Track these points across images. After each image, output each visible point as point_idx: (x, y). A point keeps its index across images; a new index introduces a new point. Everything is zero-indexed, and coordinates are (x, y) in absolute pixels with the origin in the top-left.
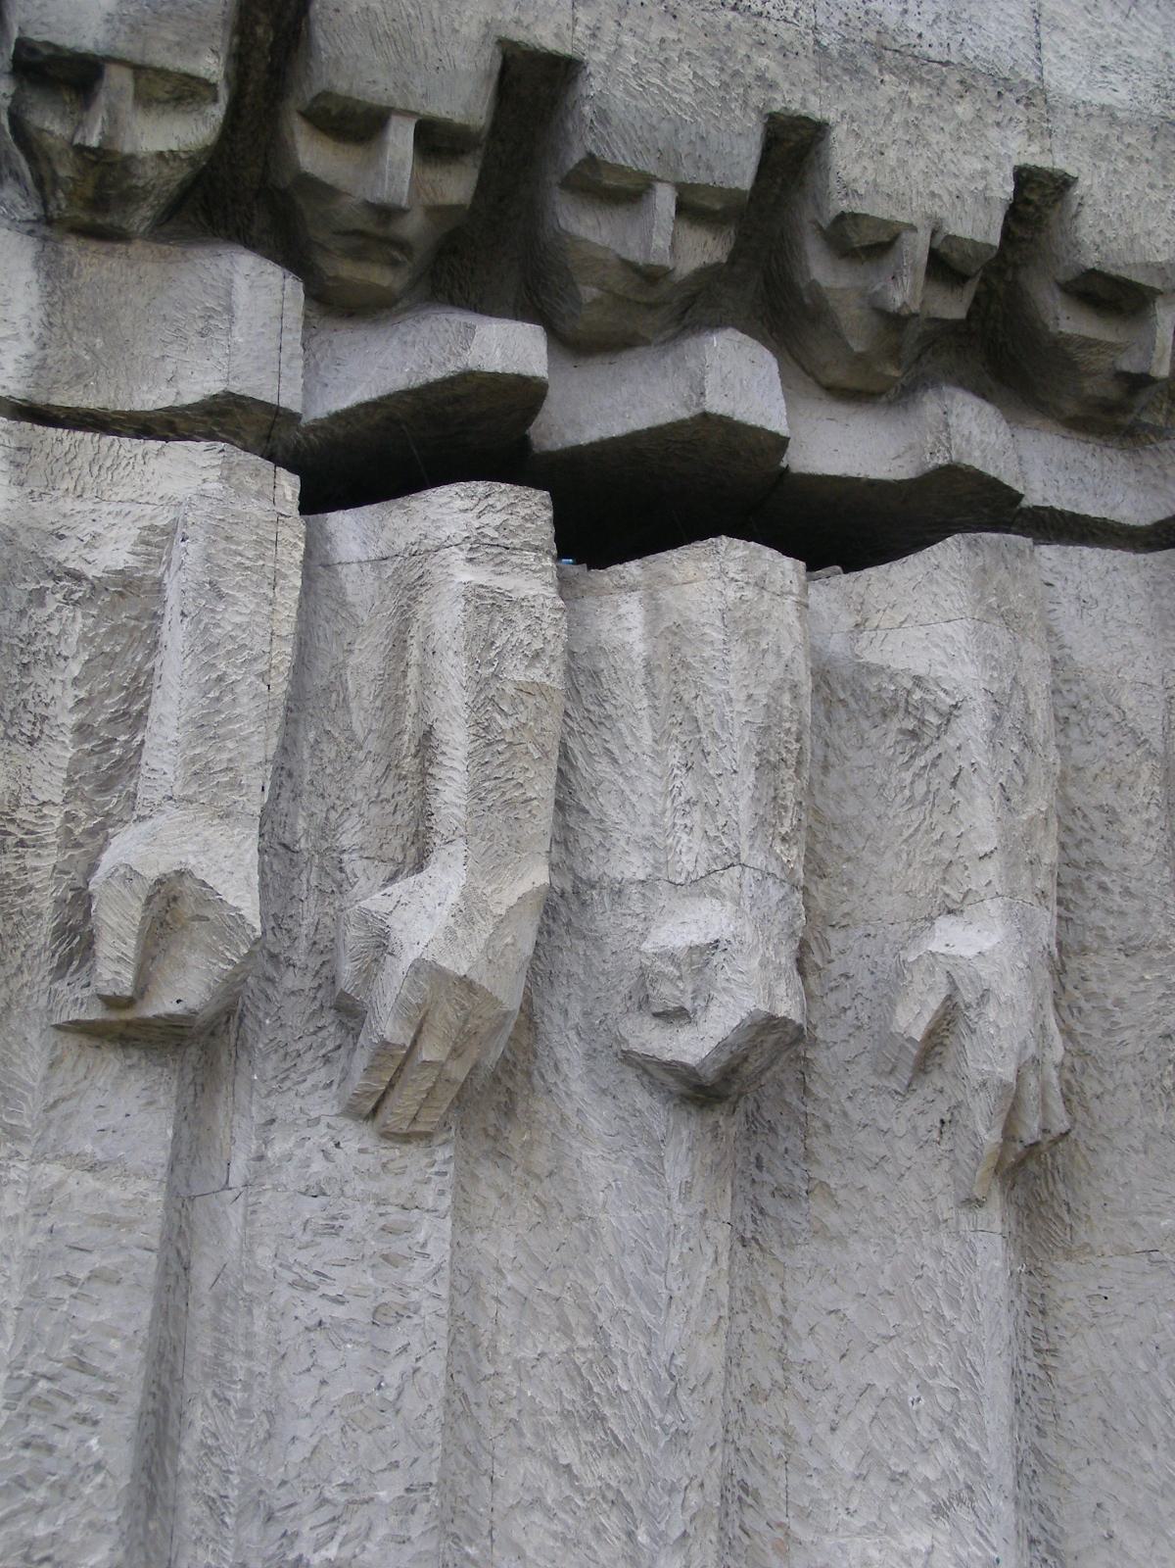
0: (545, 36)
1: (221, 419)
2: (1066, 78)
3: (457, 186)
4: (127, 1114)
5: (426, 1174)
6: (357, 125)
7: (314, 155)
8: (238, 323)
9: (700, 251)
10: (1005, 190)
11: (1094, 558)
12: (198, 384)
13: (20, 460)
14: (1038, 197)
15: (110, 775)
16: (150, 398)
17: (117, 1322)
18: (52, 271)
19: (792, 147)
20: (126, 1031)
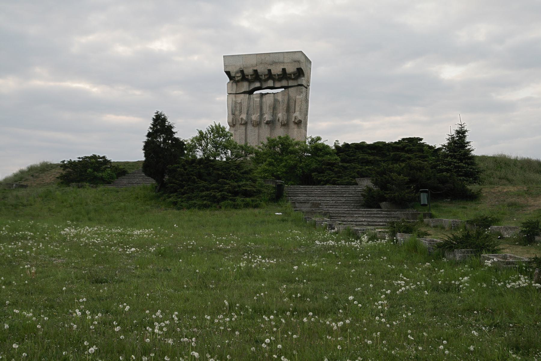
0: (255, 69)
1: (244, 93)
2: (285, 61)
3: (254, 76)
4: (243, 128)
5: (256, 129)
6: (248, 75)
7: (246, 77)
8: (245, 86)
9: (266, 77)
10: (281, 70)
11: (292, 88)
12: (243, 91)
13: (235, 97)
14: (284, 70)
15: (241, 112)
16: (241, 92)
17: (243, 136)
18: (237, 85)
19: (269, 71)
20: (241, 124)
